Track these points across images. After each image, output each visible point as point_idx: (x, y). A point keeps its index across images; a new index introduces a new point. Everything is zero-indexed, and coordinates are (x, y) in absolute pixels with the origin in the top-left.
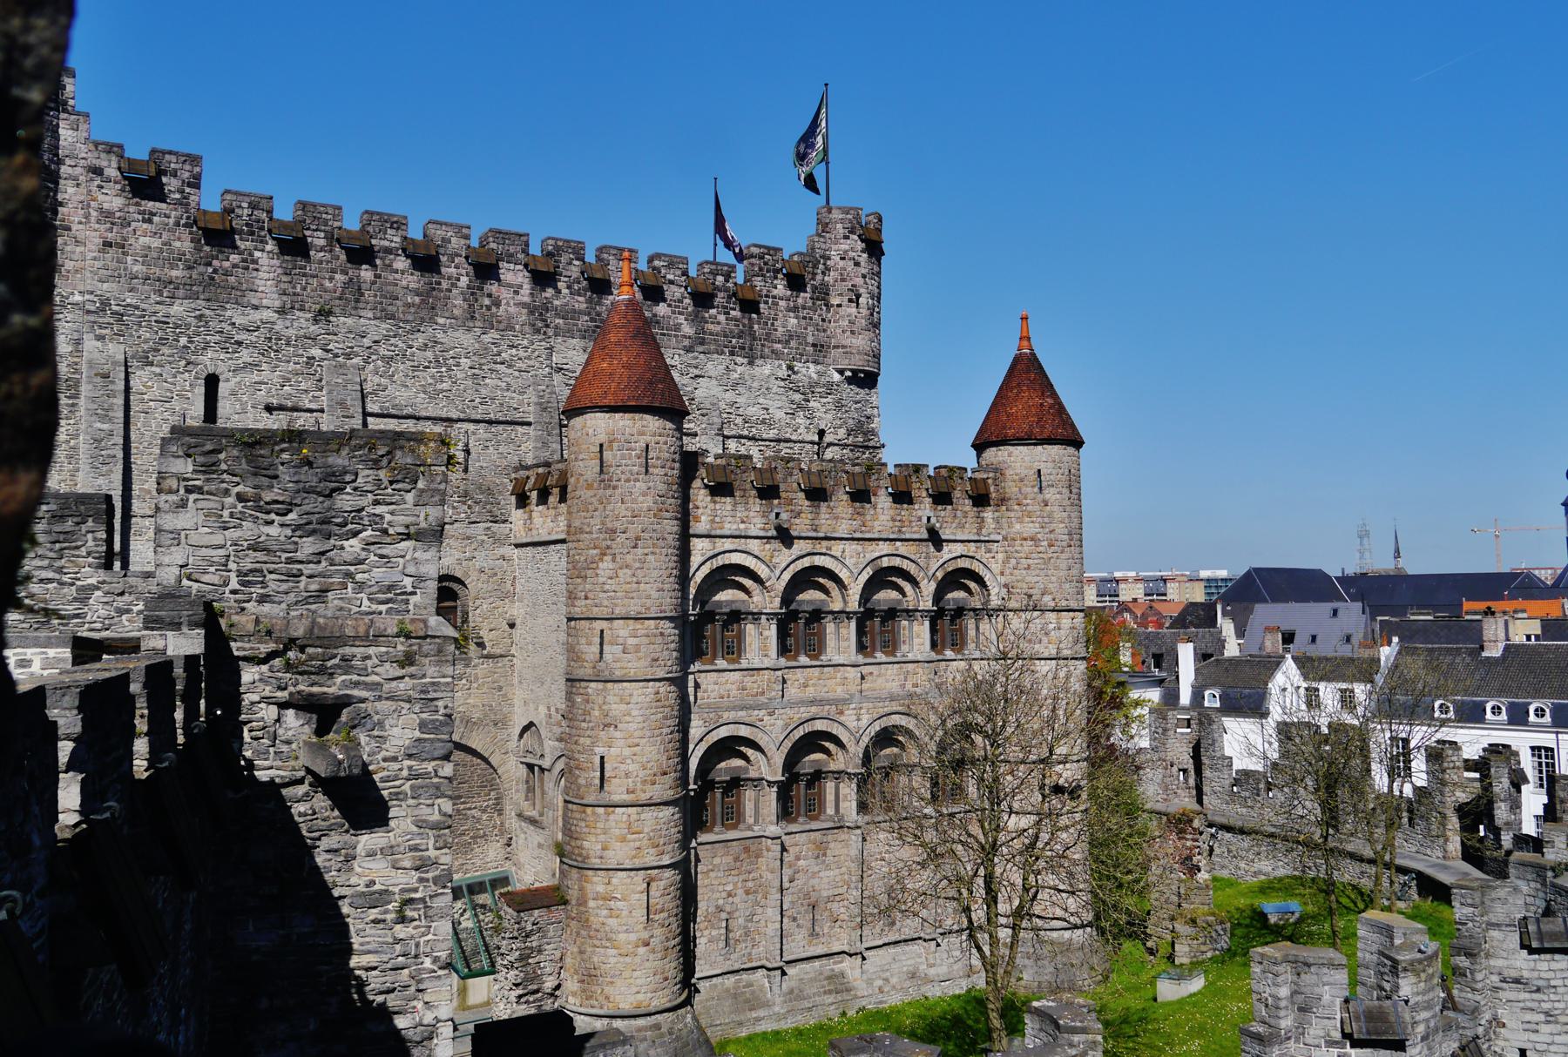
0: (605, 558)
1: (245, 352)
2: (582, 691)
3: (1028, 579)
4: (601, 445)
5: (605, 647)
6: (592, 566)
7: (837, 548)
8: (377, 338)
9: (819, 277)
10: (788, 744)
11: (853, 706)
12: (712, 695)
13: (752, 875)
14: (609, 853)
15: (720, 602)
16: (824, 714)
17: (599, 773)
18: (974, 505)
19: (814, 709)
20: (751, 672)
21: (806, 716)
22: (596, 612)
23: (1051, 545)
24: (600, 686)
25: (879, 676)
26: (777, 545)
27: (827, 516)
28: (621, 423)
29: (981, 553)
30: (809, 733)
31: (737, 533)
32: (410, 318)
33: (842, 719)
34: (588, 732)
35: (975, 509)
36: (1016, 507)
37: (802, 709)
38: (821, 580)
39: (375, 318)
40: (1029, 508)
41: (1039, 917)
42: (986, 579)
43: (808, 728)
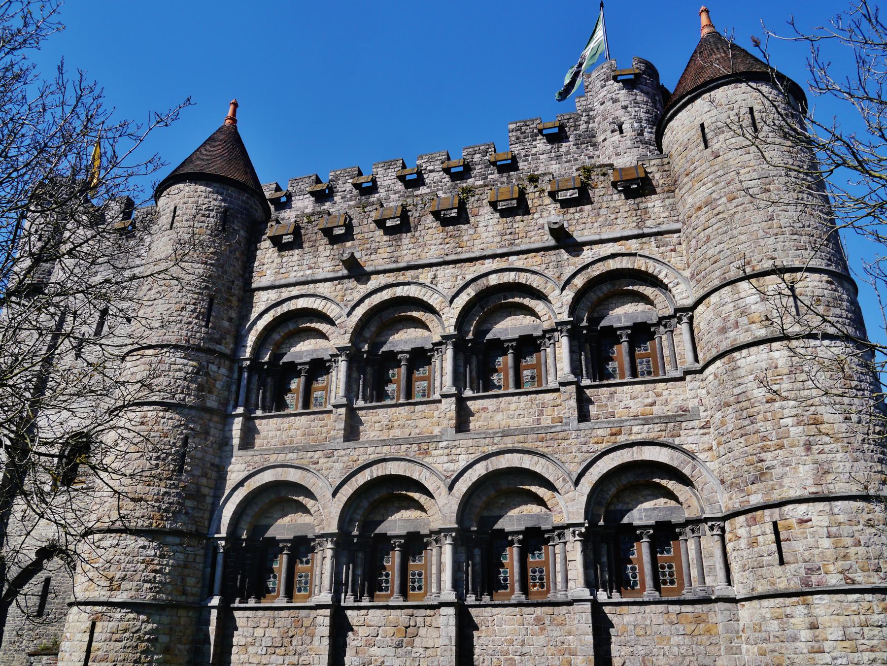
3: (710, 253)
7: (425, 276)
9: (583, 127)
10: (348, 491)
11: (442, 444)
12: (273, 442)
13: (302, 658)
15: (301, 353)
16: (401, 455)
18: (627, 198)
19: (386, 449)
20: (320, 416)
21: (373, 457)
23: (731, 200)
25: (498, 410)
26: (352, 283)
27: (411, 246)
29: (651, 247)
30: (378, 477)
31: (303, 279)
33: (427, 460)
35: (631, 201)
37: (370, 450)
38: (415, 314)
42: (661, 276)
43: (377, 471)
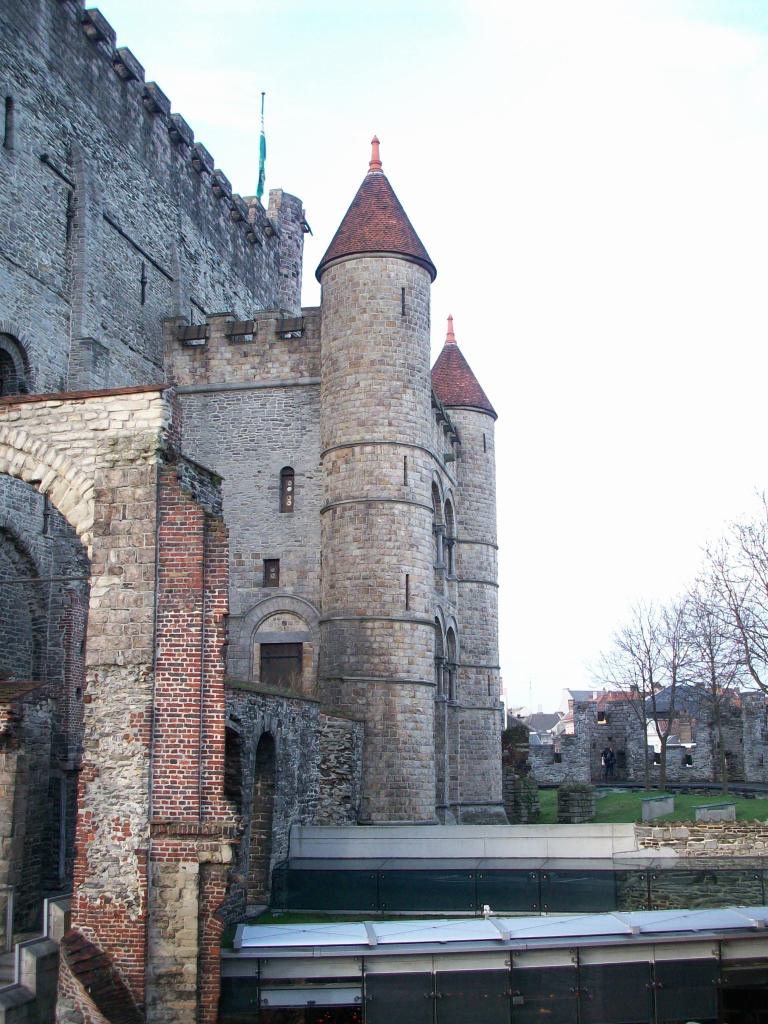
0: (408, 391)
1: (29, 90)
2: (385, 511)
4: (403, 289)
5: (408, 472)
6: (395, 396)
8: (100, 138)
14: (414, 668)
17: (405, 591)
22: (400, 438)
24: (405, 508)
28: (417, 275)
32: (116, 132)
34: (394, 551)
36: (470, 461)
39: (99, 118)
40: (479, 462)
41: (463, 805)
